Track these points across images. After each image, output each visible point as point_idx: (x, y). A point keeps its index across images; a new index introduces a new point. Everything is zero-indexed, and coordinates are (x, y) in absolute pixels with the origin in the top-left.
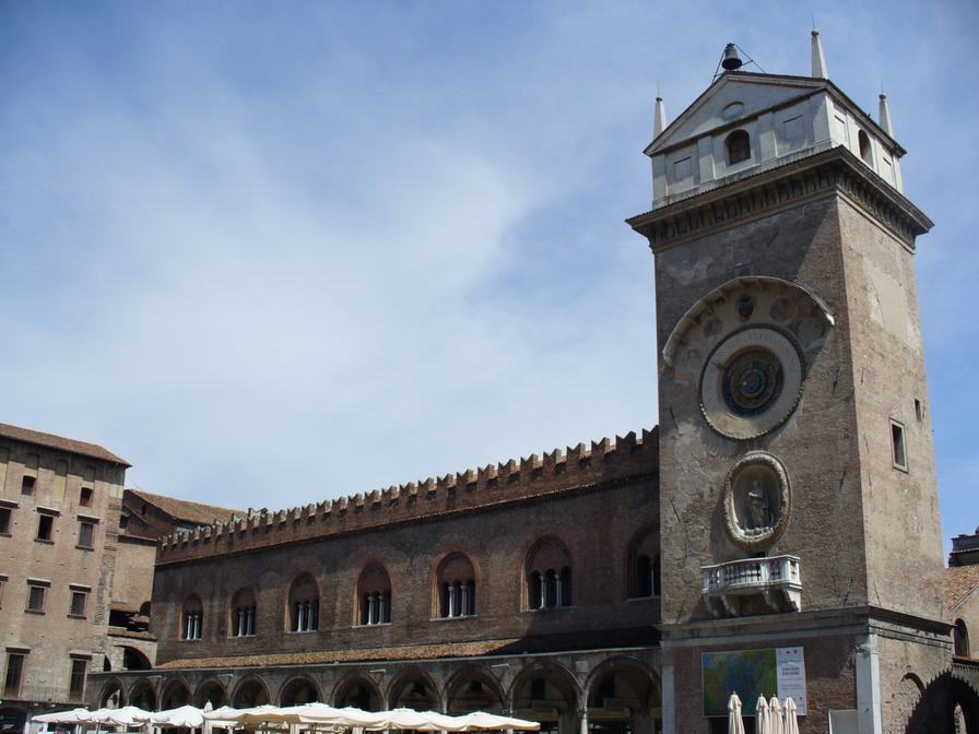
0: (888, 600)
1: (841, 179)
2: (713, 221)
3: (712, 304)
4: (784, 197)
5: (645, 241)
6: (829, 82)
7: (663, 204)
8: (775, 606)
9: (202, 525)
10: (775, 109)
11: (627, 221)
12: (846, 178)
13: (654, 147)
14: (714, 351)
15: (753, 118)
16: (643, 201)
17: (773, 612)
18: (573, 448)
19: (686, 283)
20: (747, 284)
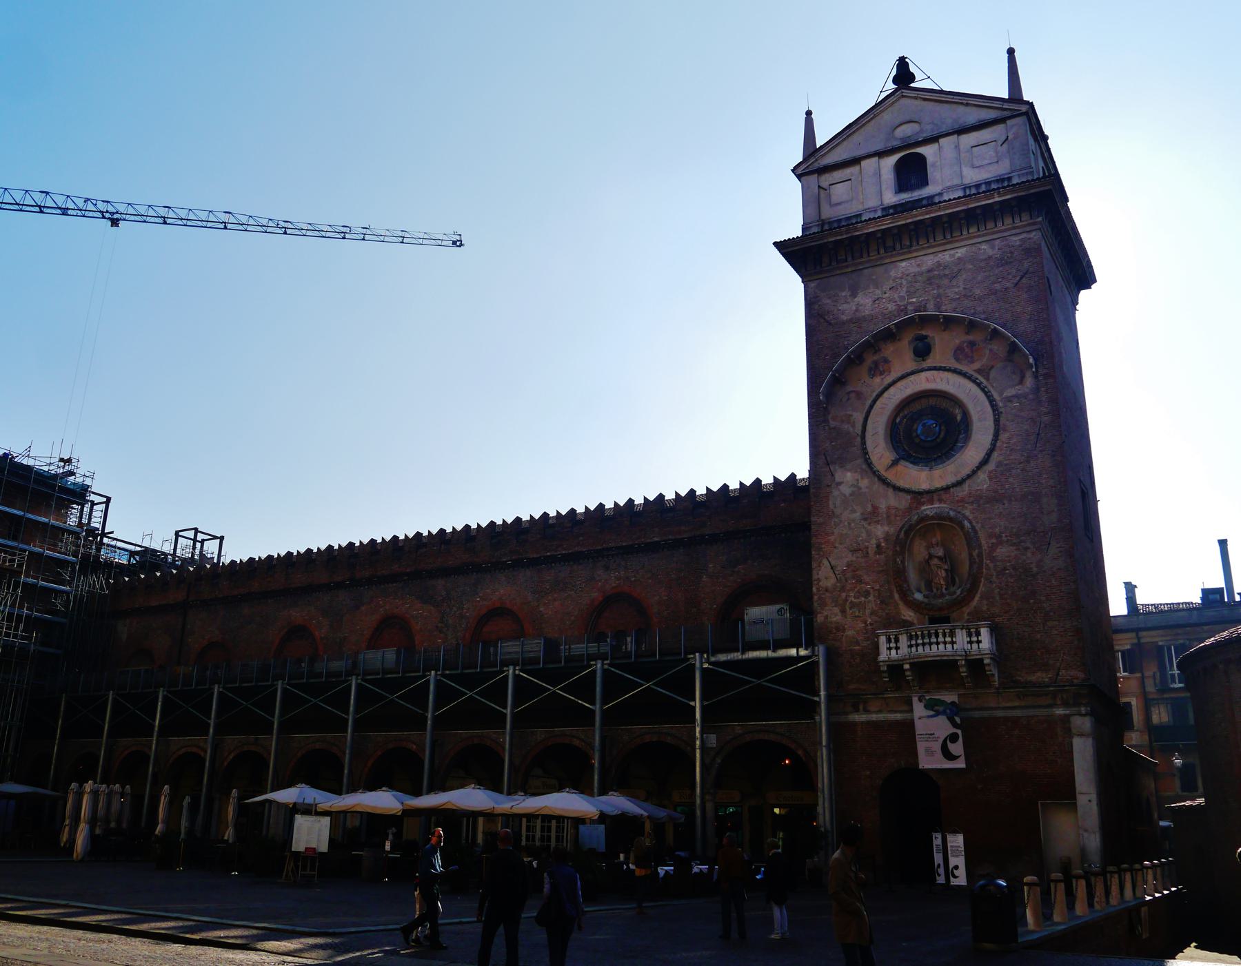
2: (882, 251)
7: (815, 230)
11: (775, 244)
15: (933, 139)
19: (845, 318)
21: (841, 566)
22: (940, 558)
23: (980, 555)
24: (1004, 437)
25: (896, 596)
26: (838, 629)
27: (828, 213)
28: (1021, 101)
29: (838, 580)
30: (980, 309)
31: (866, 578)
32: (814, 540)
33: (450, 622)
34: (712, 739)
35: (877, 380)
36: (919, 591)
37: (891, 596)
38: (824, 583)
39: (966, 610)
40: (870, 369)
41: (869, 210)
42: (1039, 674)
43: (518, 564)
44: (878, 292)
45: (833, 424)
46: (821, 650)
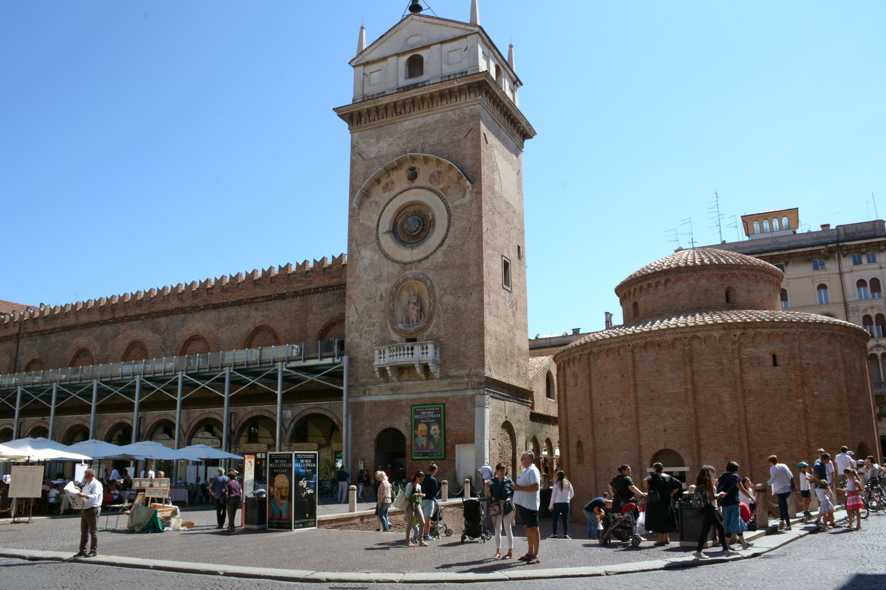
1: (484, 94)
3: (389, 170)
4: (444, 102)
5: (346, 125)
8: (423, 376)
10: (442, 43)
11: (334, 109)
12: (487, 93)
13: (355, 61)
14: (389, 202)
16: (346, 99)
17: (421, 379)
18: (283, 266)
19: (372, 156)
20: (413, 159)
22: (415, 304)
23: (434, 301)
24: (452, 230)
25: (389, 326)
26: (357, 346)
27: (370, 91)
28: (476, 25)
29: (359, 317)
32: (347, 293)
33: (169, 344)
34: (289, 414)
35: (387, 194)
37: (387, 326)
38: (351, 319)
39: (426, 334)
40: (384, 188)
41: (390, 89)
42: (461, 371)
43: (207, 307)
44: (391, 140)
45: (361, 221)
46: (345, 358)
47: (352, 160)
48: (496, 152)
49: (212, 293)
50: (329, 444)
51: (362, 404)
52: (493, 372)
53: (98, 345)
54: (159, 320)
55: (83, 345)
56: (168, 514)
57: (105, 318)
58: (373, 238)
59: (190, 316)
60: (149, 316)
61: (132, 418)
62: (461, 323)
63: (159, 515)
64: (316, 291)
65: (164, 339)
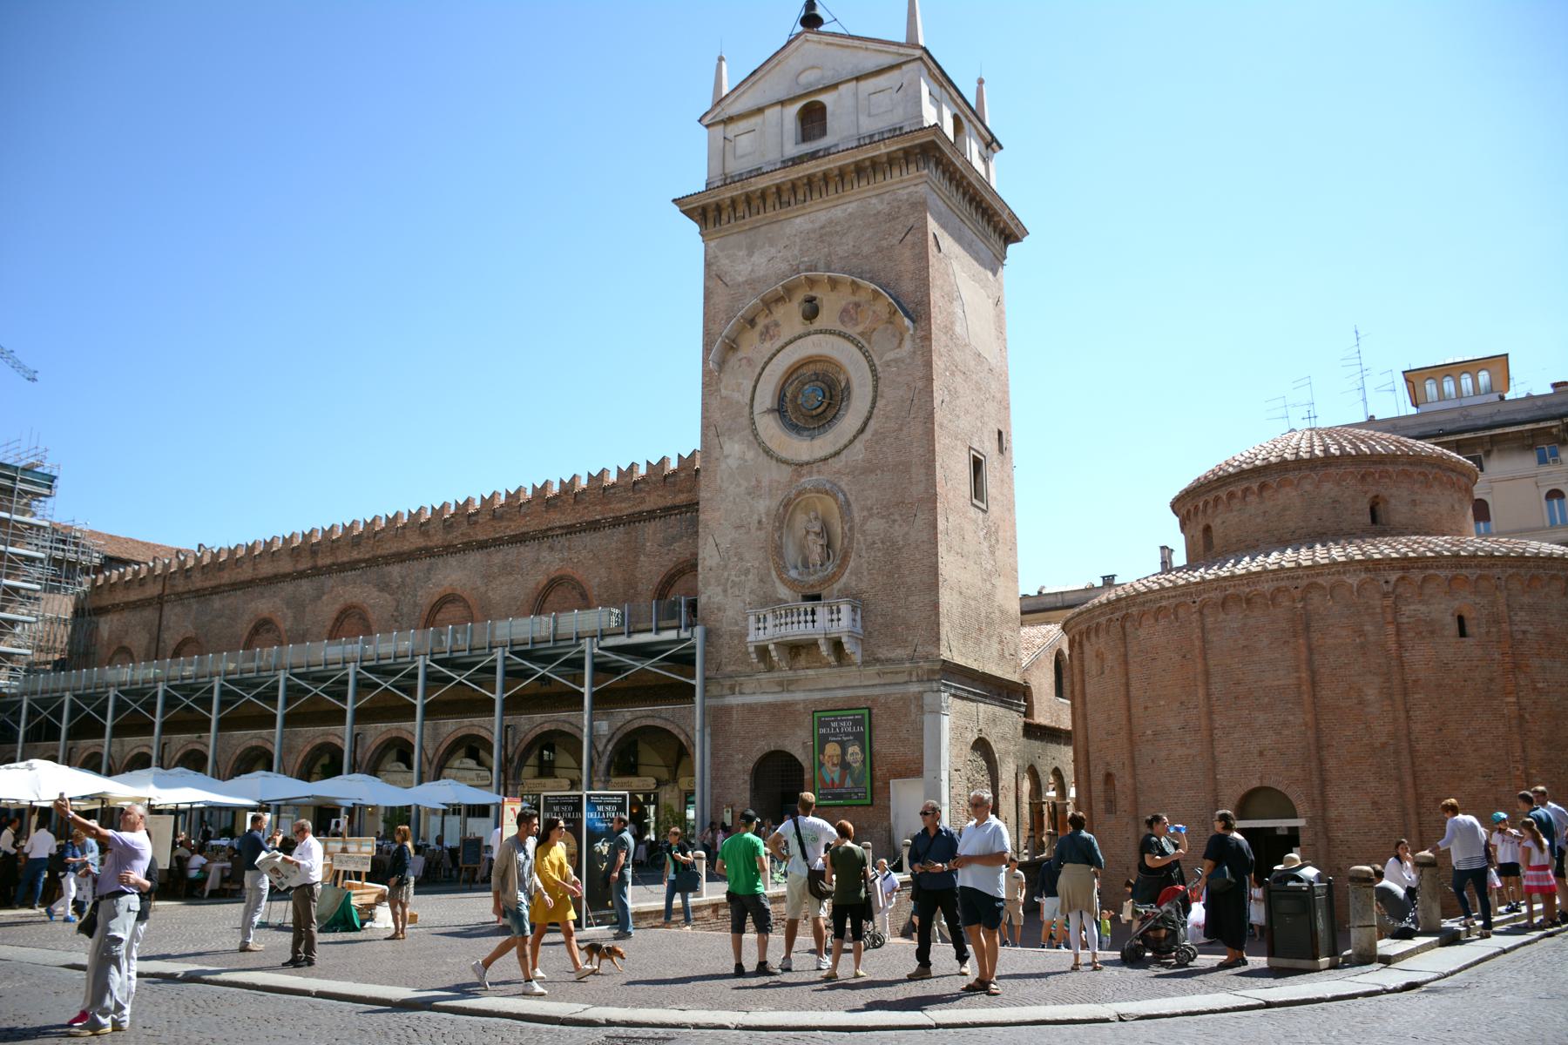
0: (962, 655)
1: (932, 165)
3: (770, 303)
4: (864, 183)
6: (925, 49)
8: (832, 659)
9: (138, 563)
10: (858, 79)
14: (771, 359)
16: (695, 181)
17: (829, 665)
19: (740, 279)
20: (812, 282)
21: (725, 544)
22: (817, 534)
23: (851, 529)
25: (774, 573)
26: (719, 609)
27: (735, 167)
28: (916, 46)
30: (866, 268)
31: (747, 556)
32: (702, 517)
34: (603, 727)
35: (767, 345)
36: (796, 567)
37: (769, 574)
39: (836, 586)
40: (762, 334)
41: (769, 163)
42: (899, 651)
43: (468, 547)
44: (773, 250)
46: (698, 630)
47: (706, 288)
48: (956, 266)
49: (476, 523)
50: (674, 779)
51: (727, 710)
52: (955, 653)
53: (290, 614)
54: (389, 568)
55: (266, 614)
56: (371, 899)
57: (301, 567)
58: (745, 421)
59: (440, 562)
60: (372, 562)
61: (343, 735)
62: (899, 567)
63: (355, 901)
64: (651, 515)
65: (398, 602)
